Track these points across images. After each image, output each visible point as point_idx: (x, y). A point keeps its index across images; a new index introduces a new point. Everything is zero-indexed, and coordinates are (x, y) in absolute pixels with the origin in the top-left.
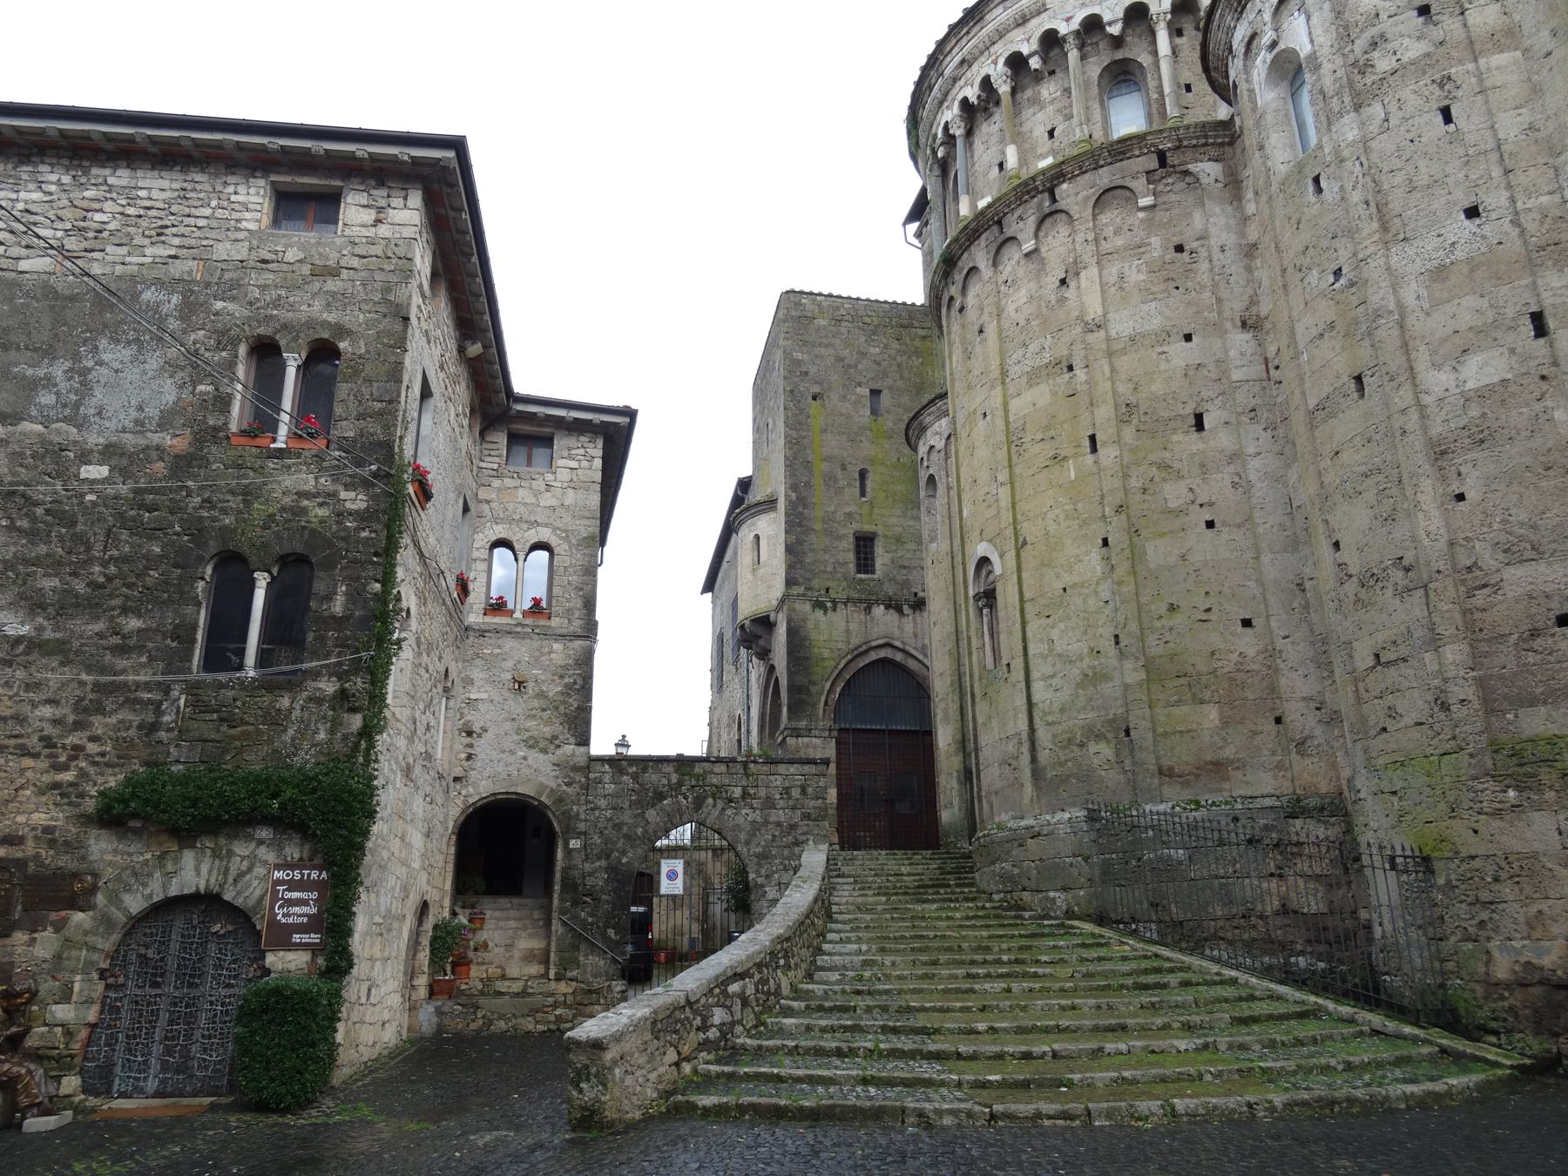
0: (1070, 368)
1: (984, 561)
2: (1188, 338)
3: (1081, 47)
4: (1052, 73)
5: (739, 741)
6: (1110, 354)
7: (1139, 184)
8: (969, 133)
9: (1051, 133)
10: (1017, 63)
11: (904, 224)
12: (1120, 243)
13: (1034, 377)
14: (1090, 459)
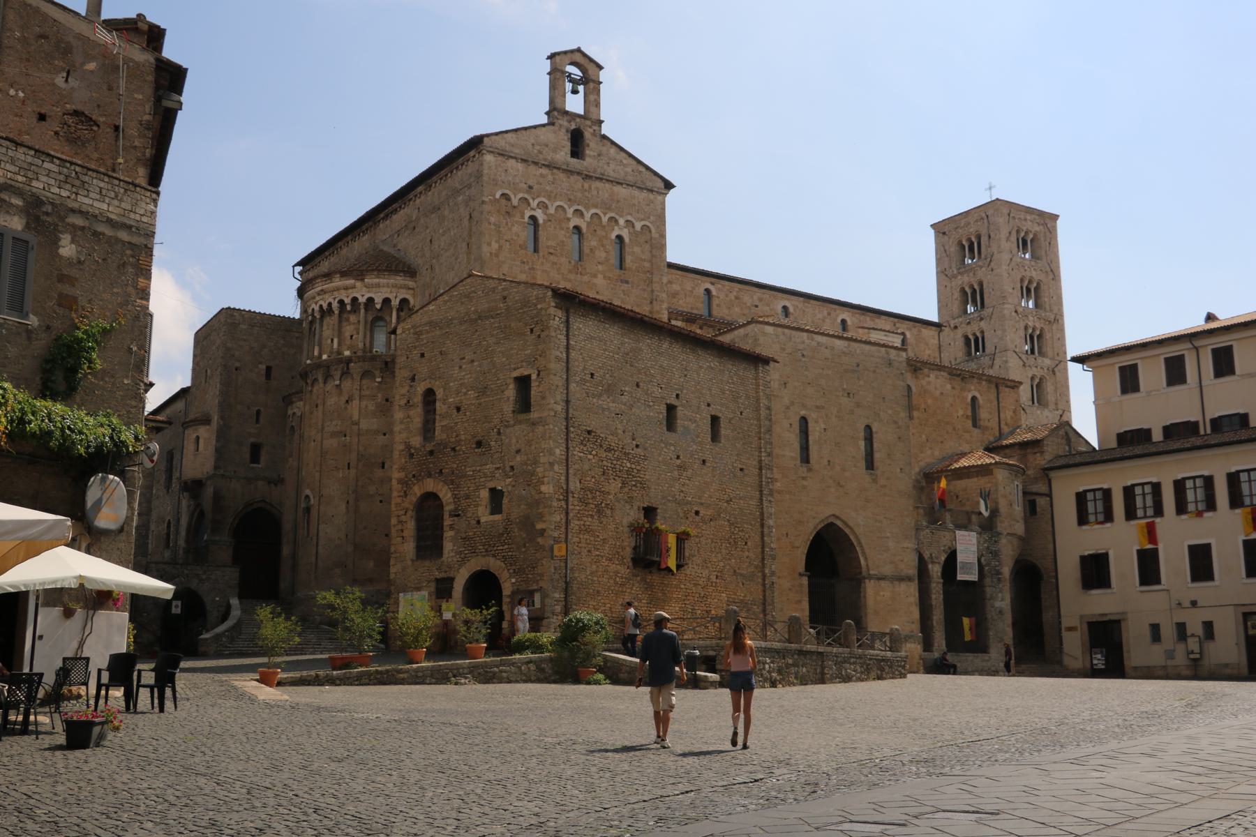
0: (345, 436)
1: (307, 497)
2: (385, 434)
3: (366, 310)
4: (355, 312)
5: (168, 535)
6: (359, 435)
7: (377, 373)
8: (322, 317)
9: (352, 337)
10: (341, 302)
11: (293, 267)
12: (368, 393)
13: (334, 434)
14: (347, 471)
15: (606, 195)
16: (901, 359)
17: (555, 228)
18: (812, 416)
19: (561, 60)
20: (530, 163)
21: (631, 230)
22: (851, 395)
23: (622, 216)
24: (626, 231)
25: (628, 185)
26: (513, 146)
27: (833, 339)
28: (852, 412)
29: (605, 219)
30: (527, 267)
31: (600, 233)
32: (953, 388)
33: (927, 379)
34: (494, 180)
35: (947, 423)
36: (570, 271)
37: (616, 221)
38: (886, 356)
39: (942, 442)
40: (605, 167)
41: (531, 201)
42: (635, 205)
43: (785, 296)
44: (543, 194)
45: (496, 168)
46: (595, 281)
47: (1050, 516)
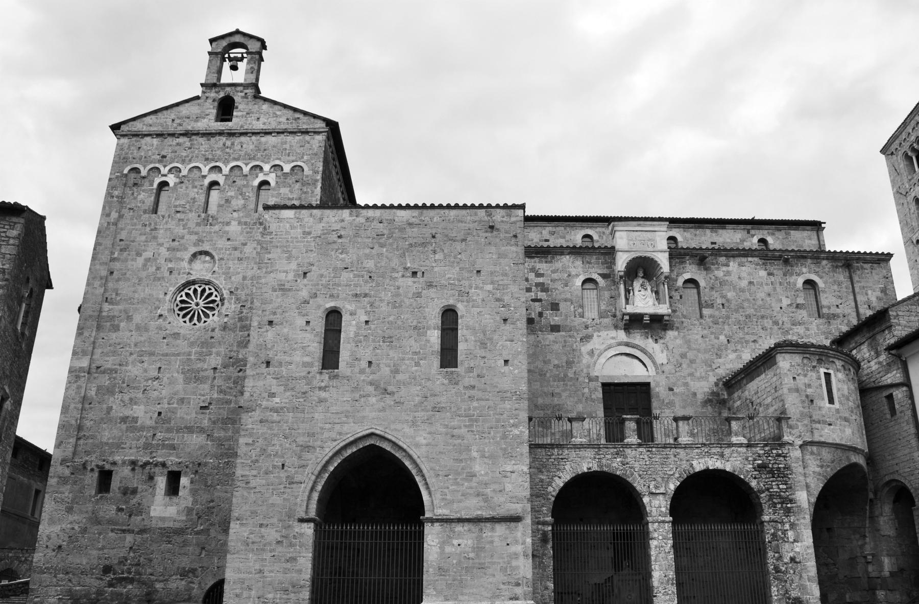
15: (252, 147)
16: (513, 219)
17: (187, 188)
18: (346, 307)
19: (217, 45)
20: (166, 136)
21: (279, 173)
22: (419, 274)
23: (266, 163)
24: (273, 175)
25: (278, 133)
26: (151, 126)
27: (394, 210)
28: (418, 295)
29: (246, 169)
30: (148, 229)
31: (240, 182)
32: (770, 274)
33: (724, 269)
34: (124, 158)
35: (763, 317)
36: (198, 224)
37: (261, 168)
38: (486, 218)
39: (754, 341)
40: (254, 122)
41: (162, 169)
42: (286, 149)
43: (585, 224)
44: (176, 160)
45: (129, 148)
46: (227, 228)
47: (909, 413)
